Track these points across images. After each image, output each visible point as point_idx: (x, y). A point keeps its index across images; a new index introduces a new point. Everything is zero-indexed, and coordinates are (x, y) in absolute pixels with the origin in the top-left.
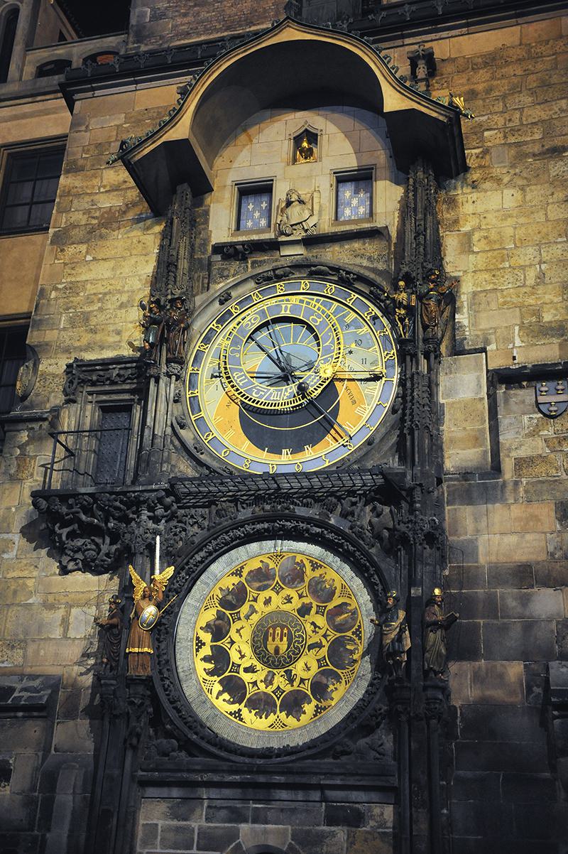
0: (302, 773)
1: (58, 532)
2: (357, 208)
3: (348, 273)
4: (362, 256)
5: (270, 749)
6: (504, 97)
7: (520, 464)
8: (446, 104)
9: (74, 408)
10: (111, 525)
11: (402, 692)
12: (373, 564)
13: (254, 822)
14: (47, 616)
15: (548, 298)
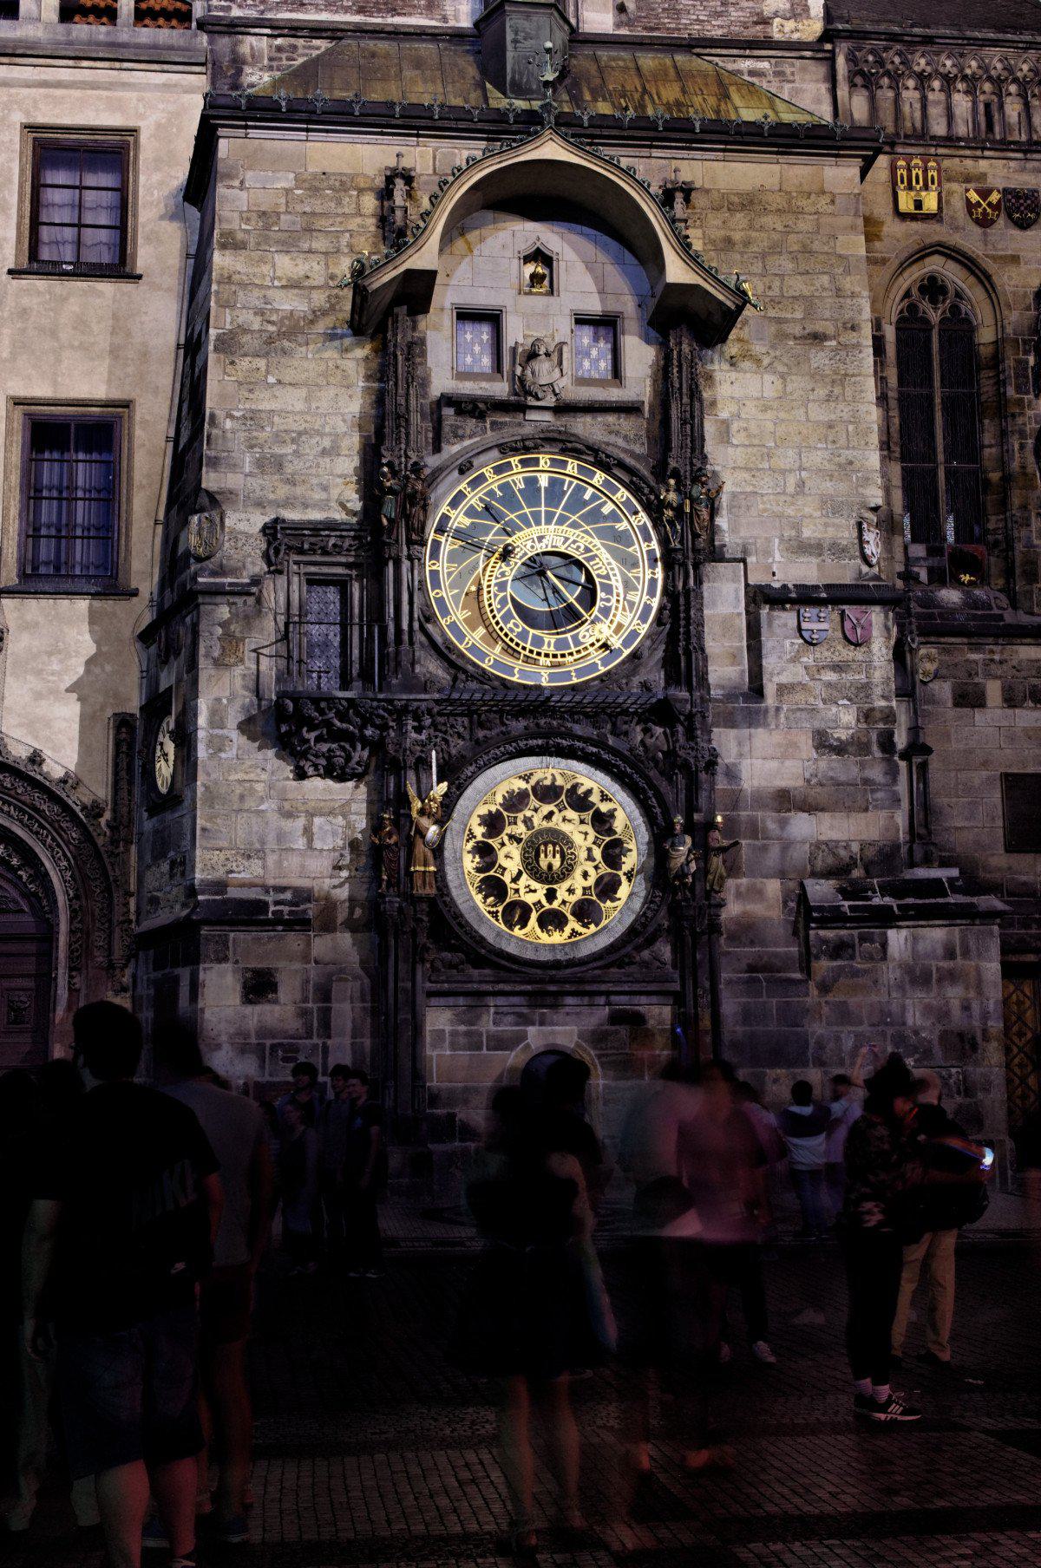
0: (594, 981)
1: (307, 736)
2: (598, 360)
3: (608, 456)
4: (617, 433)
5: (558, 962)
6: (764, 256)
7: (782, 689)
8: (732, 286)
9: (282, 580)
10: (369, 732)
11: (682, 906)
12: (652, 786)
13: (542, 1024)
14: (288, 825)
15: (807, 510)
